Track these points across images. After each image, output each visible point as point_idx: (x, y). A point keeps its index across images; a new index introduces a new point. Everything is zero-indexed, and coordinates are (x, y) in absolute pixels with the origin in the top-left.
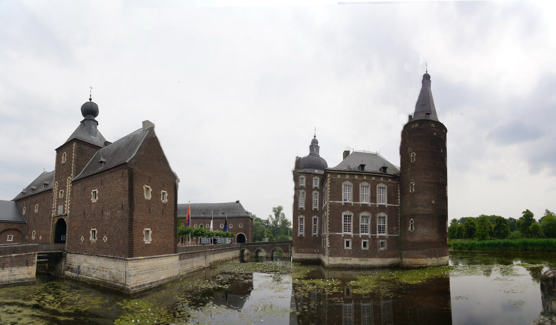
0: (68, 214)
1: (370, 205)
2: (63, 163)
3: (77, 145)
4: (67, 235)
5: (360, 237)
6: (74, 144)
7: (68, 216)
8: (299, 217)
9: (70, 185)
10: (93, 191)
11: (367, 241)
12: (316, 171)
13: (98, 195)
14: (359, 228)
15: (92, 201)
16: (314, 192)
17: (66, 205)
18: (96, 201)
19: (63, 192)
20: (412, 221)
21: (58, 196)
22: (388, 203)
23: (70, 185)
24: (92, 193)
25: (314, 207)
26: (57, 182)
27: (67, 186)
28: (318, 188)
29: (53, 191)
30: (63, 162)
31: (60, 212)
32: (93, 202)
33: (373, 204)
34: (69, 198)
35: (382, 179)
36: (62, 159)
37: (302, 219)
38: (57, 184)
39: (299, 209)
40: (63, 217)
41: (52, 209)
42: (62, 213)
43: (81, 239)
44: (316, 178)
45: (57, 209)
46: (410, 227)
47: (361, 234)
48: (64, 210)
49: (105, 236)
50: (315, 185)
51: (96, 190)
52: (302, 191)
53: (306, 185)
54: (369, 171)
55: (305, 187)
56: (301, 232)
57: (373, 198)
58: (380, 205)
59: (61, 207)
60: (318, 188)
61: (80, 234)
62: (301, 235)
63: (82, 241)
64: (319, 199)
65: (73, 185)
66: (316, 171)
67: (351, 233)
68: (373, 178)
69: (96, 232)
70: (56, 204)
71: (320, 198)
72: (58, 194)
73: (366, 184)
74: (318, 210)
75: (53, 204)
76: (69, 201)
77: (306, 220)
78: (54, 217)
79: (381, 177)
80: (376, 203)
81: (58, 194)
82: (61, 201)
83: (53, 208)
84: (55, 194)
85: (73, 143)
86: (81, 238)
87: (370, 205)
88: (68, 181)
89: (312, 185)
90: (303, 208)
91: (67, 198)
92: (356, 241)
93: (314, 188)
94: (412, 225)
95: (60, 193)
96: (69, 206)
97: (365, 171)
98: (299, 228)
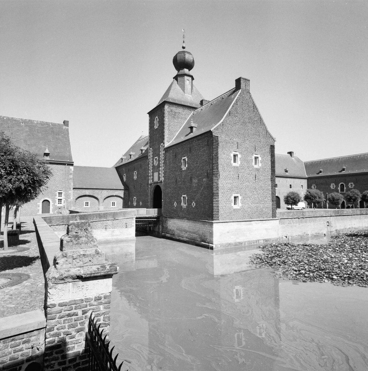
0: (163, 181)
2: (156, 128)
3: (168, 107)
4: (162, 200)
6: (166, 107)
7: (163, 183)
9: (163, 152)
10: (183, 158)
13: (187, 162)
15: (182, 169)
17: (160, 172)
18: (186, 169)
19: (157, 159)
21: (153, 163)
23: (163, 152)
24: (182, 161)
26: (151, 149)
27: (161, 153)
29: (149, 158)
30: (156, 127)
31: (156, 179)
32: (183, 169)
34: (163, 165)
36: (154, 124)
38: (152, 150)
40: (159, 184)
41: (149, 176)
42: (157, 180)
43: (175, 205)
45: (153, 176)
48: (159, 178)
49: (194, 202)
51: (186, 157)
59: (156, 174)
61: (173, 200)
63: (175, 206)
65: (166, 152)
69: (186, 199)
70: (152, 171)
72: (153, 162)
75: (150, 172)
76: (163, 168)
78: (151, 184)
81: (153, 161)
82: (156, 169)
83: (150, 175)
84: (151, 160)
85: (164, 107)
86: (175, 203)
88: (161, 148)
91: (161, 165)
95: (155, 160)
96: (163, 173)
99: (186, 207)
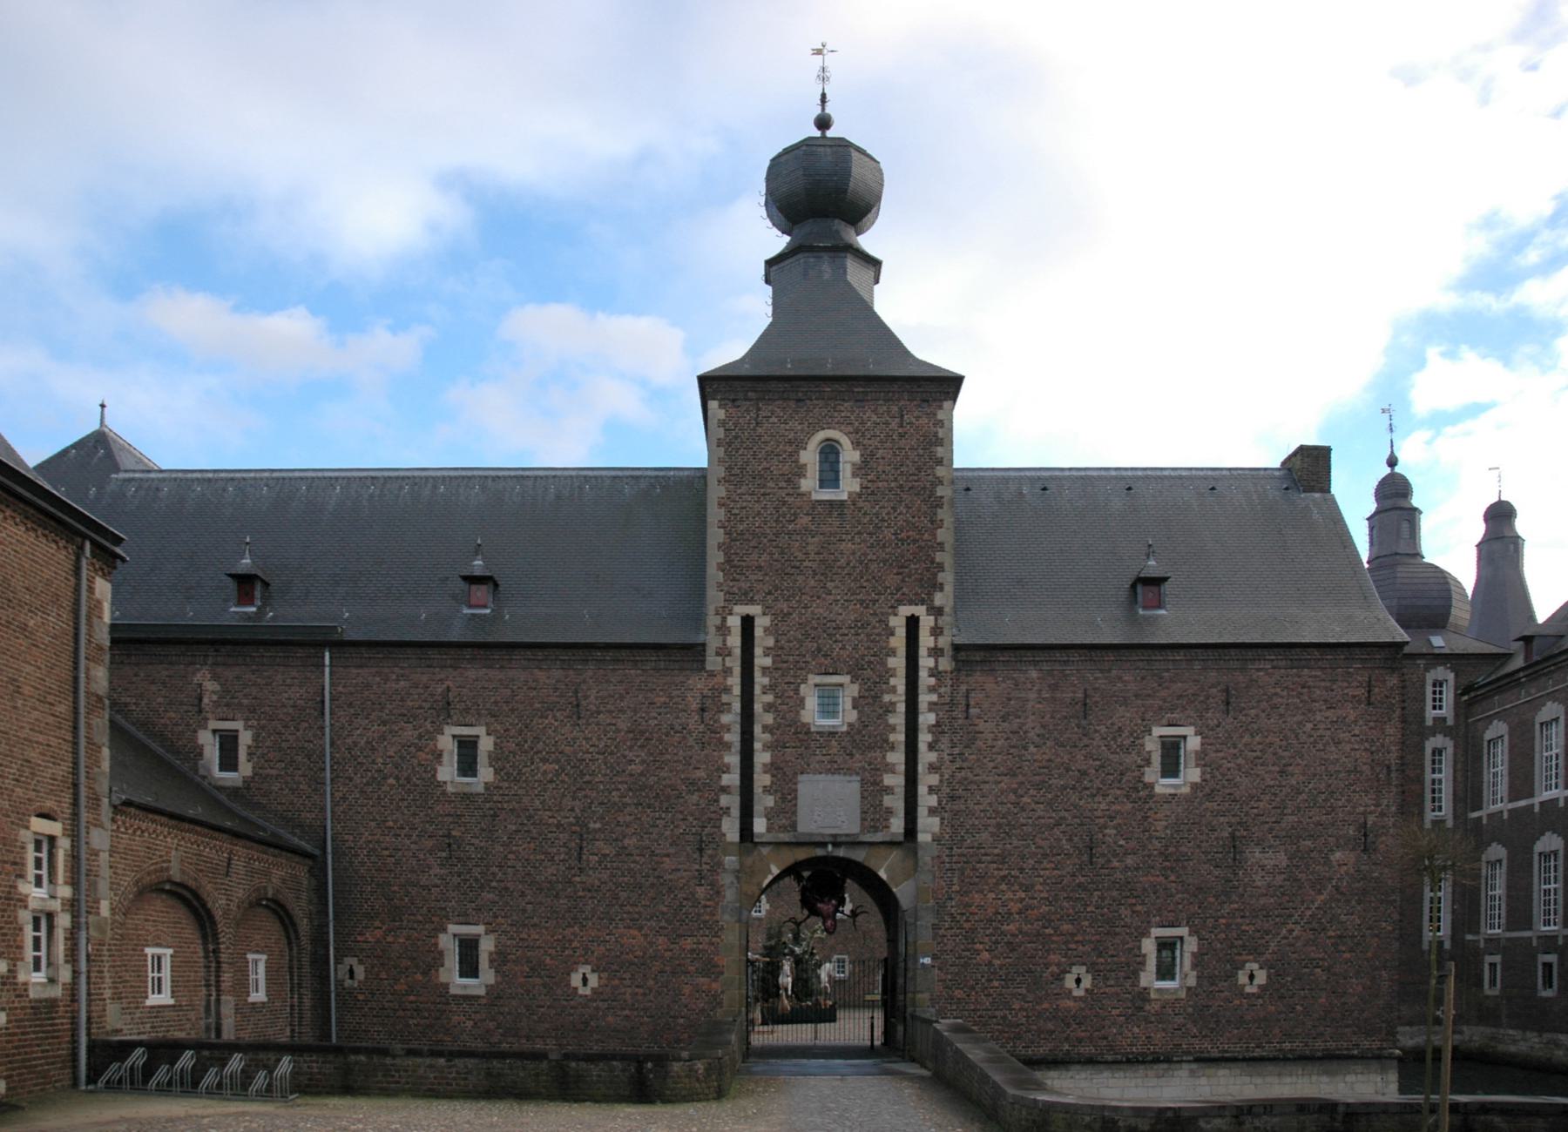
12: (1437, 641)
16: (1431, 744)
50: (1434, 708)
60: (1450, 722)
64: (1455, 771)
71: (1459, 766)
89: (1423, 710)
93: (1429, 722)
99: (1183, 994)
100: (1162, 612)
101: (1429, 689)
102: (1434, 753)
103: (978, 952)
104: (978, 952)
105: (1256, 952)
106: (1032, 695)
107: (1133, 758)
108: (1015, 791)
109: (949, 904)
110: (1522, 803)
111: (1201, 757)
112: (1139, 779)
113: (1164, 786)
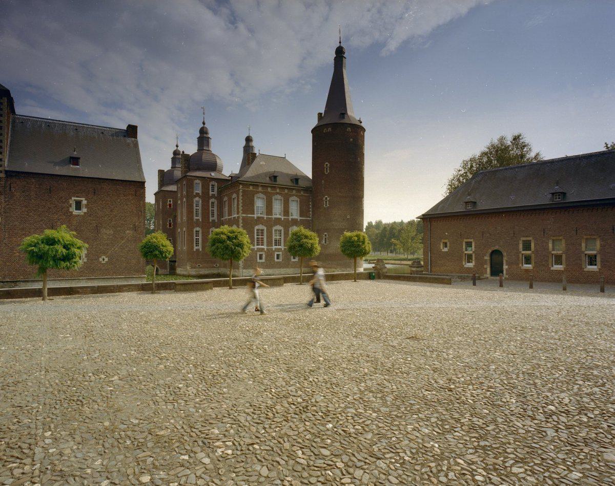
1: (283, 219)
5: (274, 250)
8: (195, 230)
11: (280, 253)
14: (272, 241)
16: (212, 200)
20: (326, 235)
22: (300, 217)
25: (211, 219)
28: (216, 196)
33: (286, 217)
35: (294, 192)
37: (198, 232)
39: (195, 220)
44: (213, 183)
46: (324, 240)
47: (274, 247)
52: (197, 199)
53: (202, 193)
54: (281, 183)
55: (201, 195)
56: (196, 246)
57: (286, 212)
58: (292, 219)
60: (216, 196)
62: (198, 250)
66: (213, 174)
67: (265, 247)
68: (286, 191)
73: (279, 197)
74: (216, 221)
77: (202, 233)
79: (293, 189)
80: (289, 216)
87: (283, 219)
90: (199, 219)
92: (270, 254)
94: (325, 238)
97: (277, 183)
98: (195, 243)
100: (78, 167)
101: (211, 187)
102: (212, 203)
103: (15, 253)
104: (15, 253)
105: (104, 254)
106: (33, 186)
107: (66, 205)
108: (27, 211)
109: (4, 240)
110: (230, 217)
111: (87, 206)
112: (68, 210)
113: (76, 212)
